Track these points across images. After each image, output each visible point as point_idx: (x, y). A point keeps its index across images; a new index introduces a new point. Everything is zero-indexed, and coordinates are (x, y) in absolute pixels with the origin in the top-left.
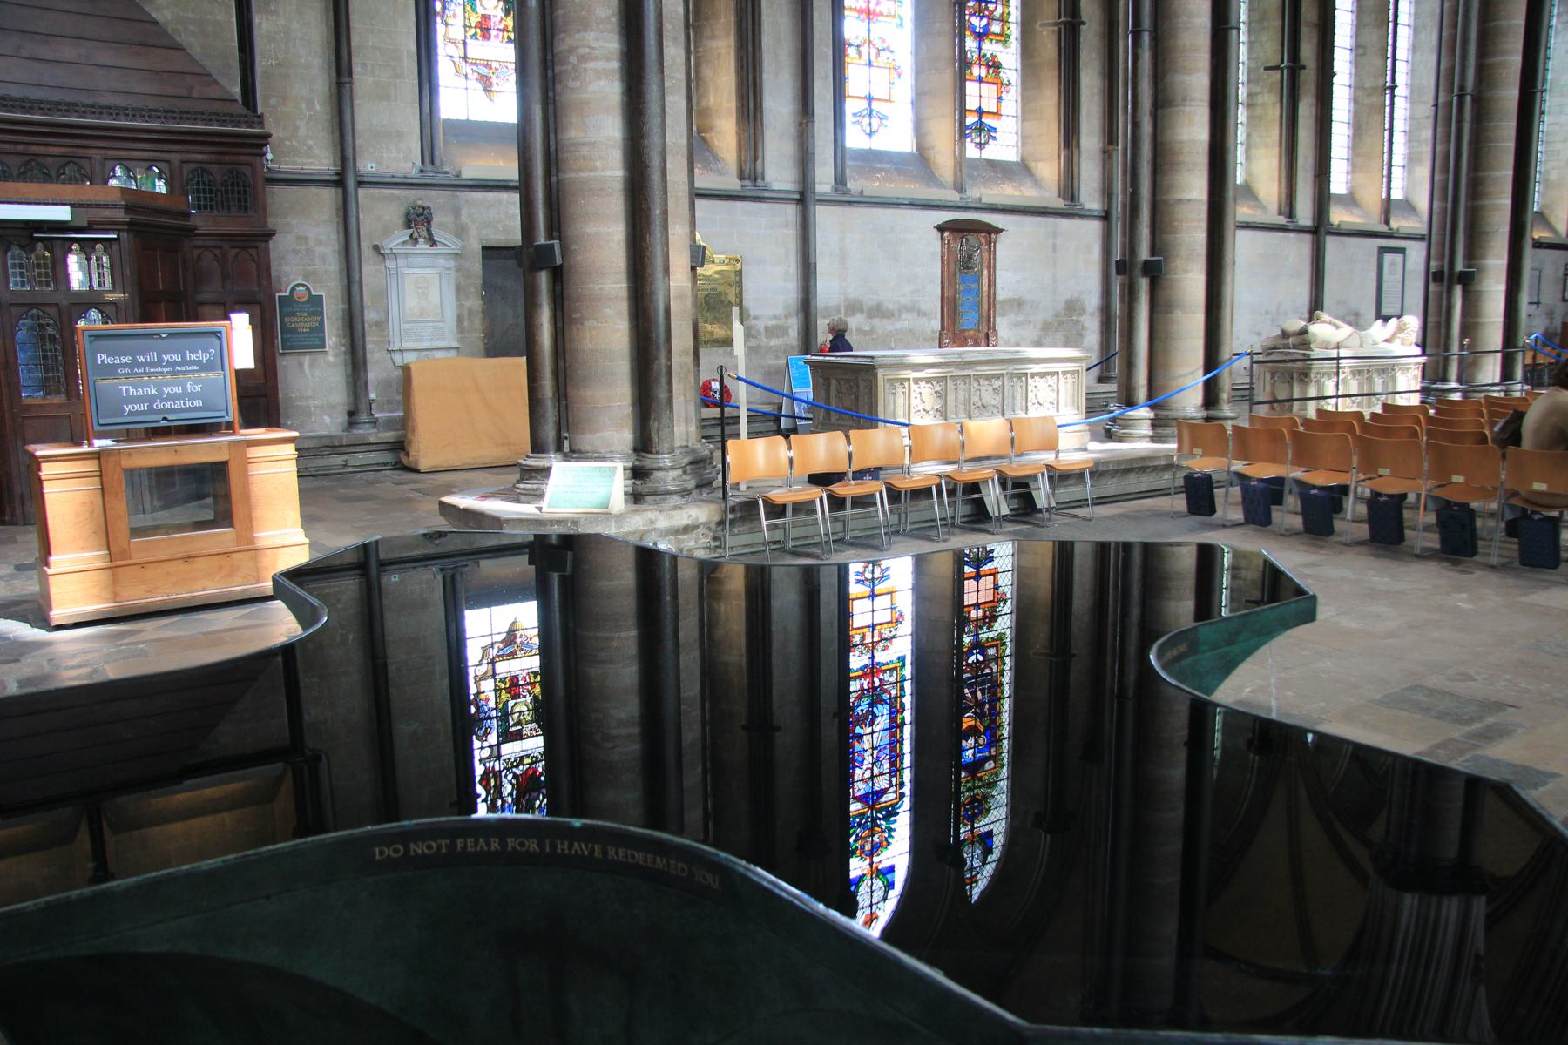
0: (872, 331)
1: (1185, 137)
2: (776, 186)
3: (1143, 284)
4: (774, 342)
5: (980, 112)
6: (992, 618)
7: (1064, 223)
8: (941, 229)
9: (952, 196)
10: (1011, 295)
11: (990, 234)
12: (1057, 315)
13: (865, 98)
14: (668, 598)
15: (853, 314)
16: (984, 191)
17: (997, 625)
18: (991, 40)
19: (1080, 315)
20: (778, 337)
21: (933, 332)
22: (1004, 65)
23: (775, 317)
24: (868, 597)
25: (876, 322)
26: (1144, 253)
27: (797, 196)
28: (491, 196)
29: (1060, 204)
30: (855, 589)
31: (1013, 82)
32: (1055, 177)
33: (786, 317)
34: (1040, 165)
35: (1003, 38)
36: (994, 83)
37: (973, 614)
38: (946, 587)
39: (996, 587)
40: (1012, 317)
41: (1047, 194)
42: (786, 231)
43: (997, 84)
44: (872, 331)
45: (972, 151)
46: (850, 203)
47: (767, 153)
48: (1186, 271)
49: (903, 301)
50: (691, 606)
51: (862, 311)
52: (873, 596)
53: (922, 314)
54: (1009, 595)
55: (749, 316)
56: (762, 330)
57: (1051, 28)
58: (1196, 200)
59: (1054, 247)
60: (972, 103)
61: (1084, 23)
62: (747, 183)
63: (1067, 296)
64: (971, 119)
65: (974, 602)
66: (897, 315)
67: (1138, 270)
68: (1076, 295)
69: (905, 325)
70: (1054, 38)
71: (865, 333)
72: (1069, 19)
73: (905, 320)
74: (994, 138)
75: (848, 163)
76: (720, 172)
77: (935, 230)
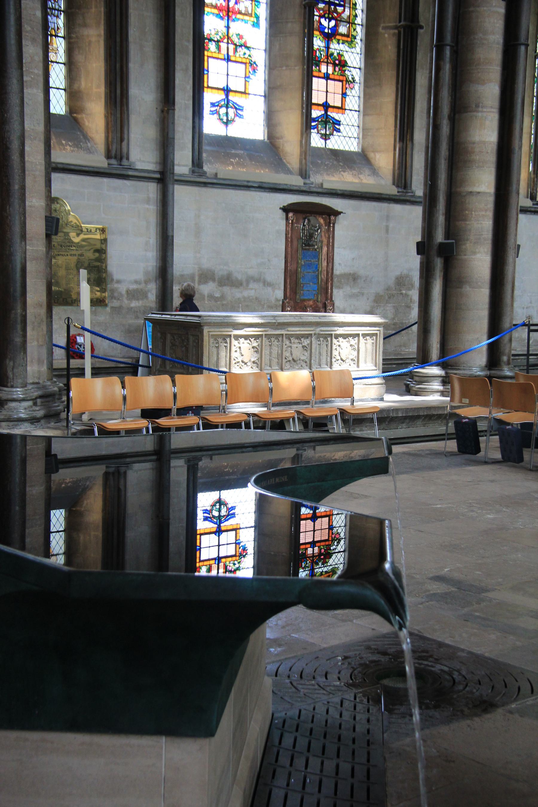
0: (223, 297)
1: (477, 139)
2: (139, 166)
3: (439, 263)
4: (134, 304)
5: (326, 106)
6: (326, 555)
7: (397, 208)
8: (286, 210)
9: (297, 181)
10: (347, 270)
11: (329, 215)
12: (388, 289)
13: (223, 89)
14: (17, 508)
15: (206, 282)
16: (327, 178)
17: (331, 561)
18: (339, 40)
19: (409, 289)
20: (138, 300)
21: (277, 300)
22: (349, 64)
23: (136, 282)
24: (215, 533)
25: (226, 289)
26: (440, 237)
27: (158, 176)
29: (393, 191)
30: (202, 525)
31: (357, 79)
32: (391, 167)
33: (146, 282)
34: (378, 156)
35: (349, 39)
36: (339, 81)
37: (310, 551)
38: (285, 523)
39: (331, 528)
40: (348, 289)
41: (383, 182)
42: (147, 206)
44: (223, 297)
45: (316, 141)
46: (205, 184)
47: (132, 136)
48: (475, 253)
49: (251, 272)
50: (37, 517)
51: (214, 280)
52: (219, 532)
53: (267, 284)
54: (342, 535)
55: (112, 280)
56: (124, 292)
57: (392, 31)
58: (485, 193)
60: (318, 97)
61: (422, 27)
62: (113, 161)
63: (398, 273)
64: (316, 113)
65: (311, 540)
66: (244, 284)
67: (434, 252)
68: (405, 272)
69: (252, 293)
70: (394, 40)
71: (216, 299)
72: (408, 23)
73: (252, 289)
74: (338, 131)
75: (205, 147)
76: (89, 151)
77: (281, 211)
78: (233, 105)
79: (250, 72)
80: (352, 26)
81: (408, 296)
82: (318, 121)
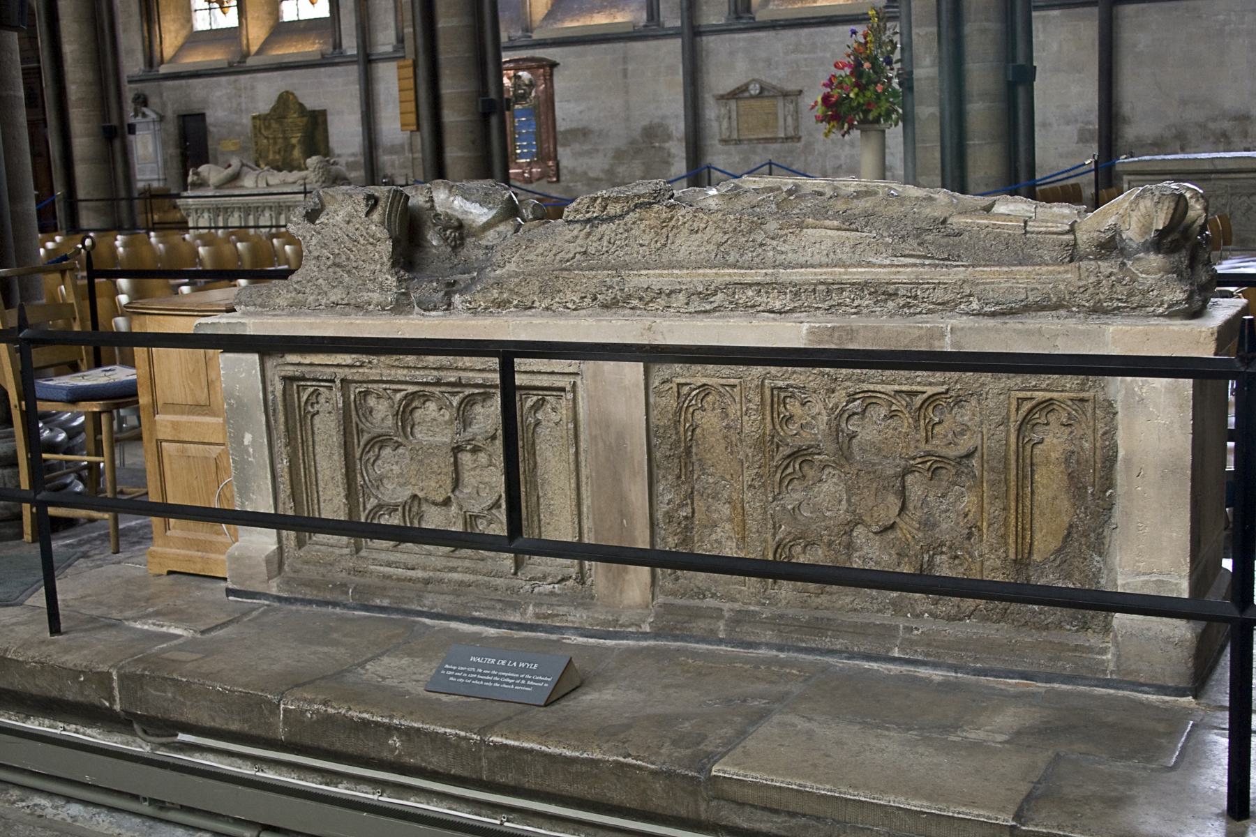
12: (633, 142)
19: (665, 141)
28: (177, 82)
40: (577, 147)
59: (625, 74)
63: (645, 123)
68: (656, 121)
81: (664, 149)
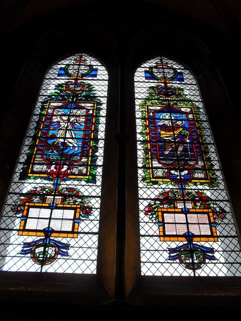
13: (44, 231)
31: (227, 209)
43: (208, 213)
78: (55, 244)
79: (80, 215)
80: (209, 172)
82: (179, 251)
